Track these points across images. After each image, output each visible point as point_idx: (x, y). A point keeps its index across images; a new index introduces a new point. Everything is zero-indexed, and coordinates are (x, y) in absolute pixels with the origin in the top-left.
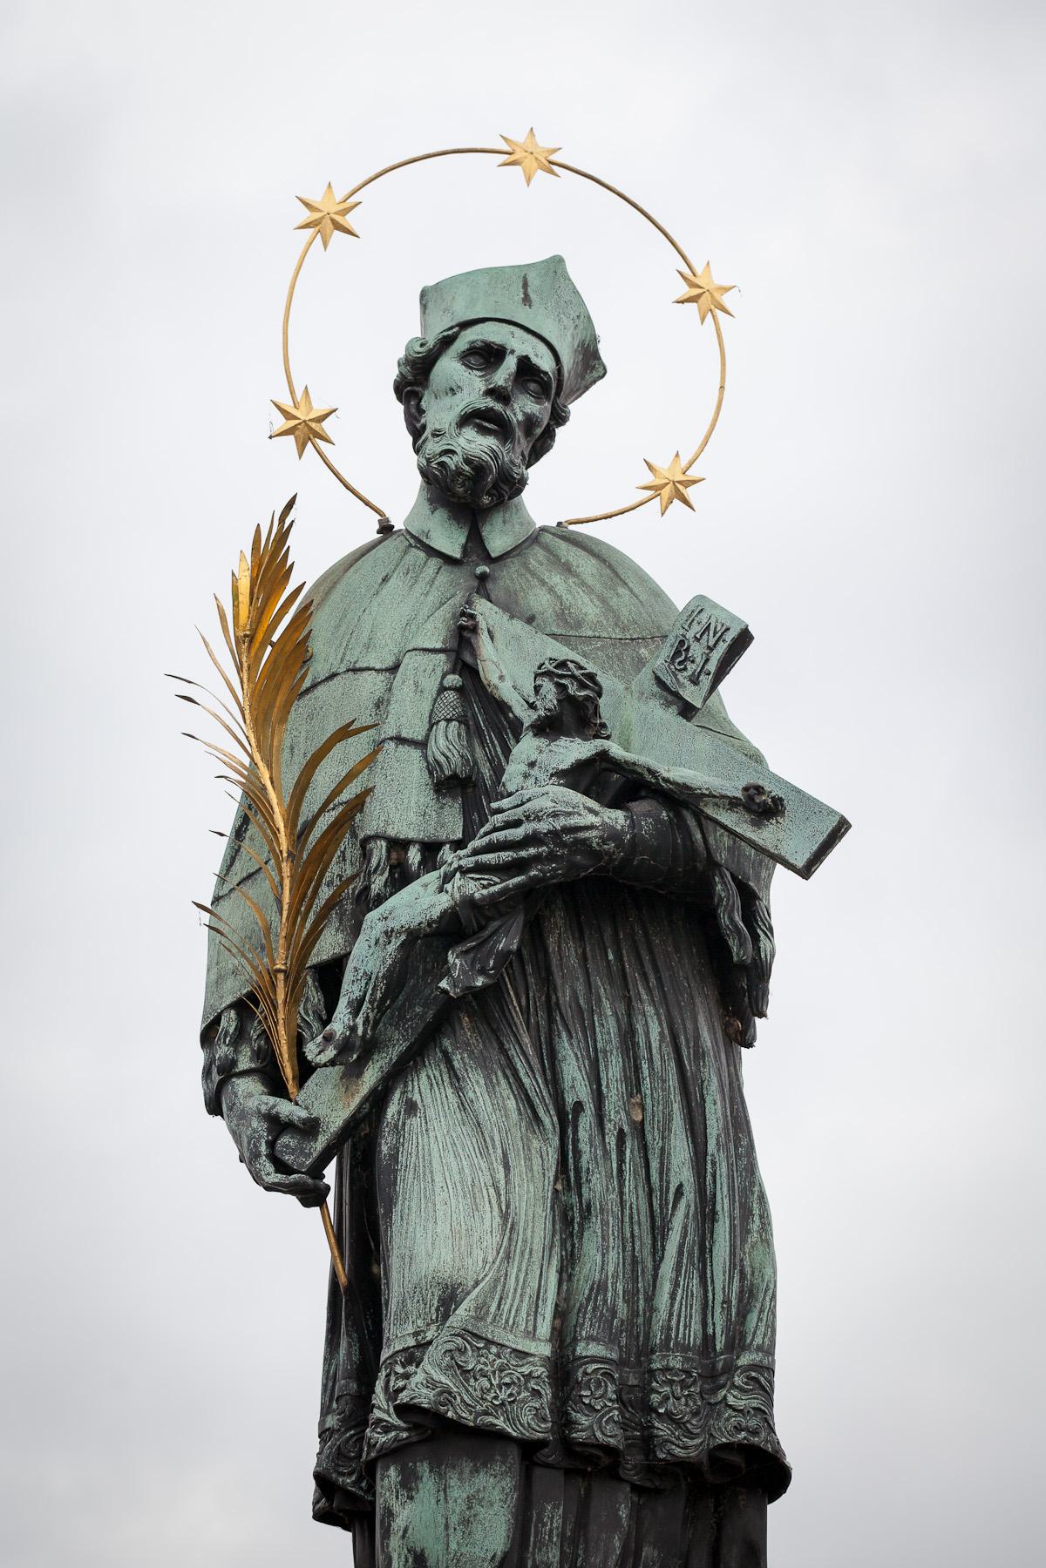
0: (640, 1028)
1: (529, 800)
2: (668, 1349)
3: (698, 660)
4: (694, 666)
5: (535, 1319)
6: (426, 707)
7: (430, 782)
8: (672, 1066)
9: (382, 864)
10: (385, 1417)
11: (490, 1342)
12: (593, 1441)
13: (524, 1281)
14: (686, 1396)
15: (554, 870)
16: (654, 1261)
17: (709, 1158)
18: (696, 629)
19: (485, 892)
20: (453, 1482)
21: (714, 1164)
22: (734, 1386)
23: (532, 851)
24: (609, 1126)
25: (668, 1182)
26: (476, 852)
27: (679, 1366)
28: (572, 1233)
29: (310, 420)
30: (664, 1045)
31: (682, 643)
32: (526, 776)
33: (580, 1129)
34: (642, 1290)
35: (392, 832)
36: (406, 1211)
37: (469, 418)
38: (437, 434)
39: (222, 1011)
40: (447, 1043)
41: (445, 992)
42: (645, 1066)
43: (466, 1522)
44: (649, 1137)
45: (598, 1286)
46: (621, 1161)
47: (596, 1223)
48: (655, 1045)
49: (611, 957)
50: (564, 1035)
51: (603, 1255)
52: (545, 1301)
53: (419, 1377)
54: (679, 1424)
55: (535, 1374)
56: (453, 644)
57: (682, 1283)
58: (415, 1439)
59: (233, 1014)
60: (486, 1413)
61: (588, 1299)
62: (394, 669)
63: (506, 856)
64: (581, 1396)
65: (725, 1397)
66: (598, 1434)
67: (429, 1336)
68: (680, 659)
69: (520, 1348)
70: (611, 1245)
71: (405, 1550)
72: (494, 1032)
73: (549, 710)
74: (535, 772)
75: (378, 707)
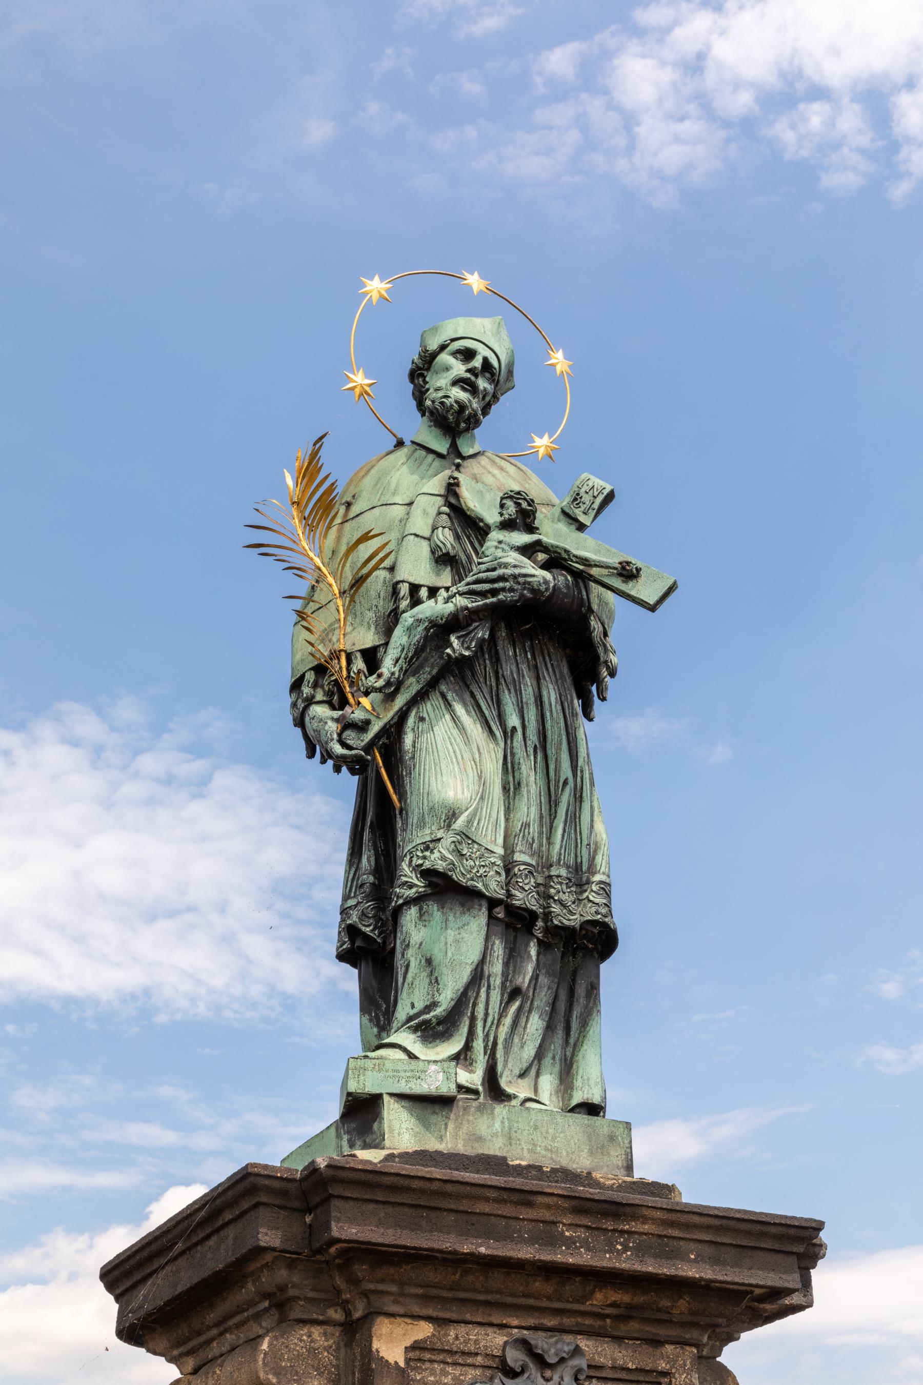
0: (545, 693)
1: (500, 558)
2: (560, 865)
3: (587, 503)
4: (585, 506)
5: (496, 835)
6: (430, 521)
7: (432, 558)
8: (561, 716)
9: (406, 595)
10: (410, 880)
11: (474, 841)
12: (524, 906)
13: (490, 814)
14: (569, 892)
15: (512, 596)
16: (550, 819)
17: (579, 768)
18: (585, 488)
19: (474, 604)
20: (451, 918)
21: (582, 771)
22: (592, 891)
23: (501, 585)
24: (529, 743)
25: (559, 777)
26: (468, 584)
27: (565, 875)
28: (509, 796)
29: (364, 384)
30: (558, 705)
31: (578, 494)
32: (497, 548)
33: (515, 741)
34: (545, 832)
35: (412, 580)
36: (422, 771)
37: (457, 382)
38: (438, 389)
39: (306, 672)
40: (443, 688)
41: (448, 655)
42: (548, 714)
43: (457, 941)
44: (549, 752)
45: (526, 825)
46: (535, 762)
47: (524, 790)
48: (553, 704)
49: (529, 656)
50: (506, 691)
51: (528, 808)
52: (500, 825)
53: (437, 854)
54: (564, 906)
55: (497, 863)
56: (442, 492)
57: (567, 830)
58: (429, 891)
59: (312, 672)
60: (472, 879)
61: (520, 830)
62: (410, 504)
63: (487, 586)
64: (517, 882)
65: (587, 897)
66: (527, 903)
67: (439, 836)
68: (577, 502)
69: (489, 848)
70: (532, 804)
71: (420, 956)
72: (468, 687)
73: (511, 515)
74: (503, 545)
75: (401, 522)
